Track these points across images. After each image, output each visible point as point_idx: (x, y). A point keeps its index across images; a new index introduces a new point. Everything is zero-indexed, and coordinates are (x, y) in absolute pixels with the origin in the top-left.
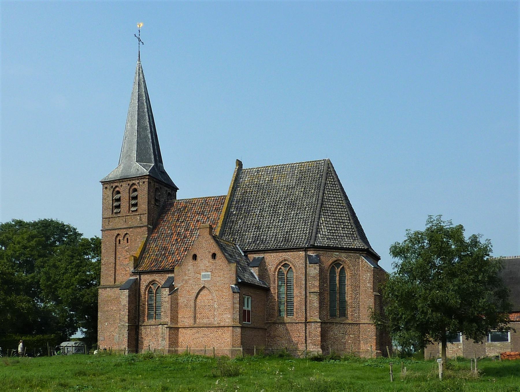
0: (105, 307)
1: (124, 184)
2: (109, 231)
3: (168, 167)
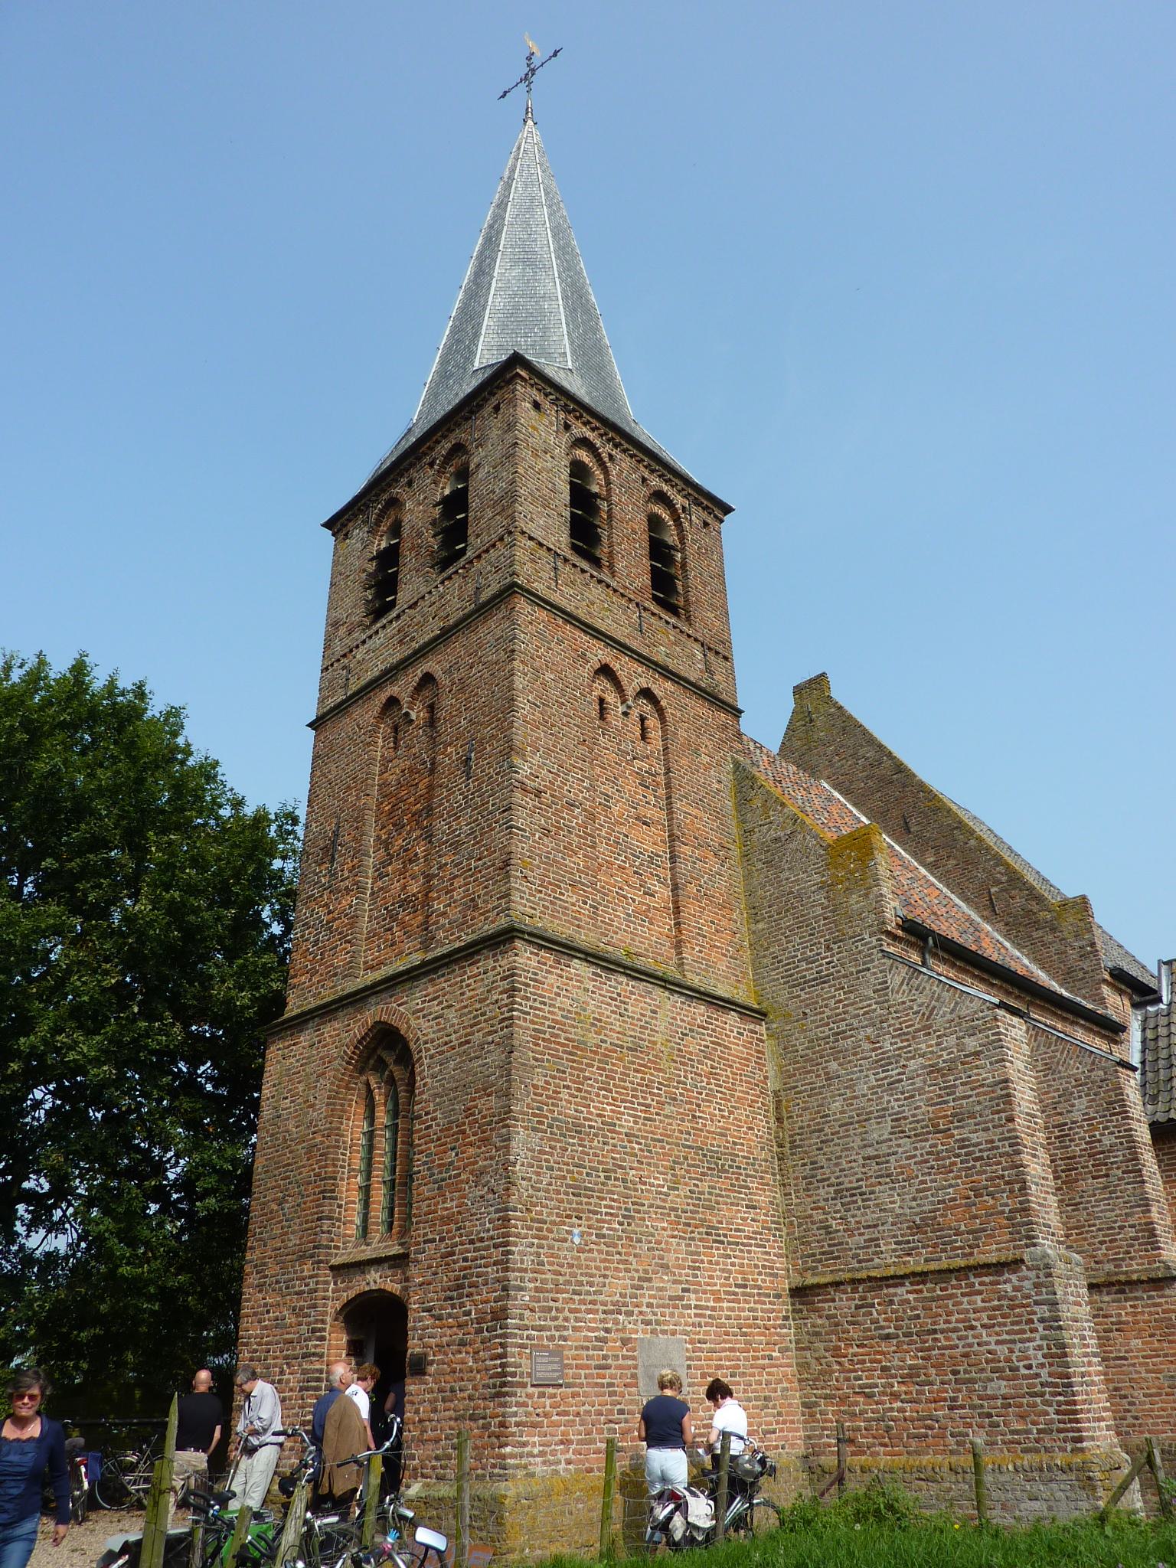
0: (564, 1094)
2: (560, 622)
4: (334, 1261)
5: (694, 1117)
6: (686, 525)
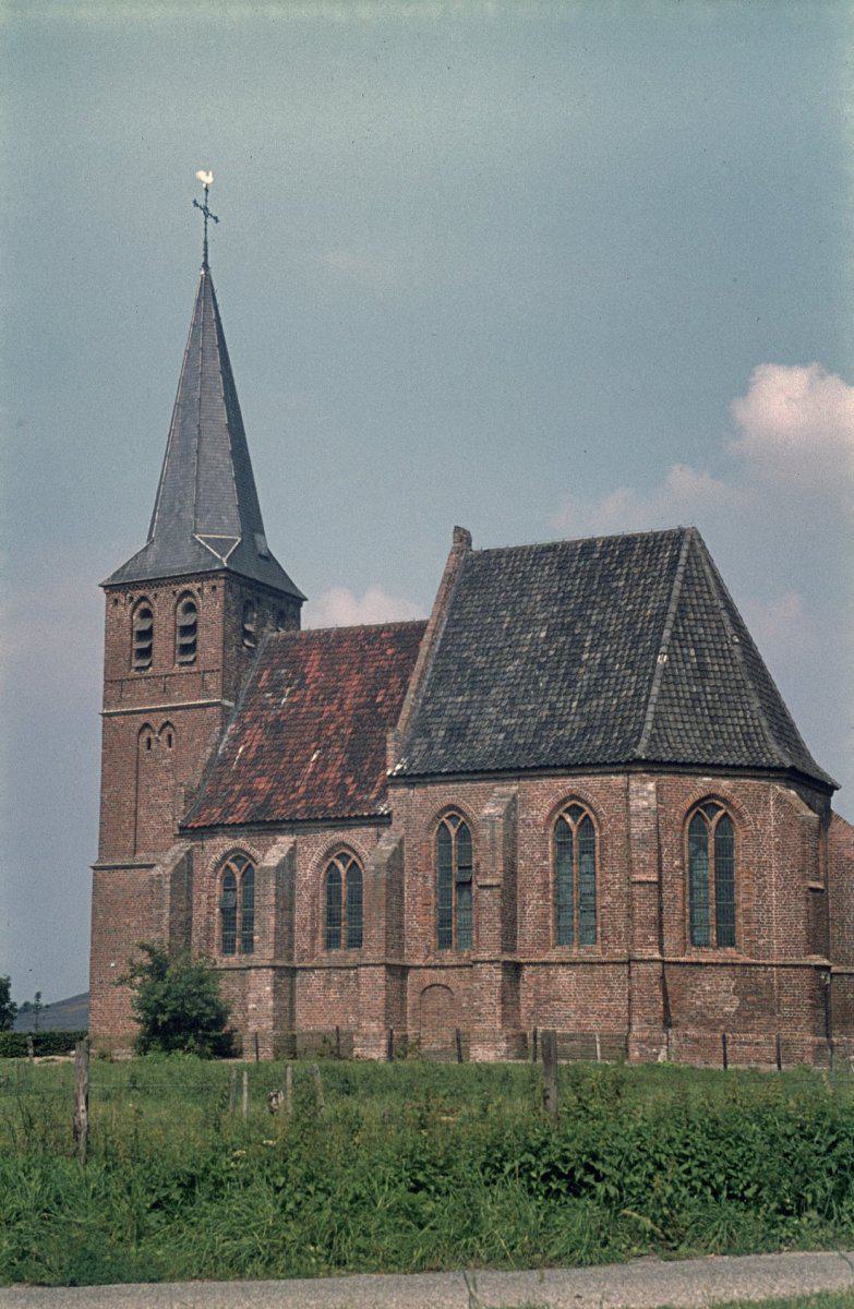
1: (163, 593)
3: (276, 541)
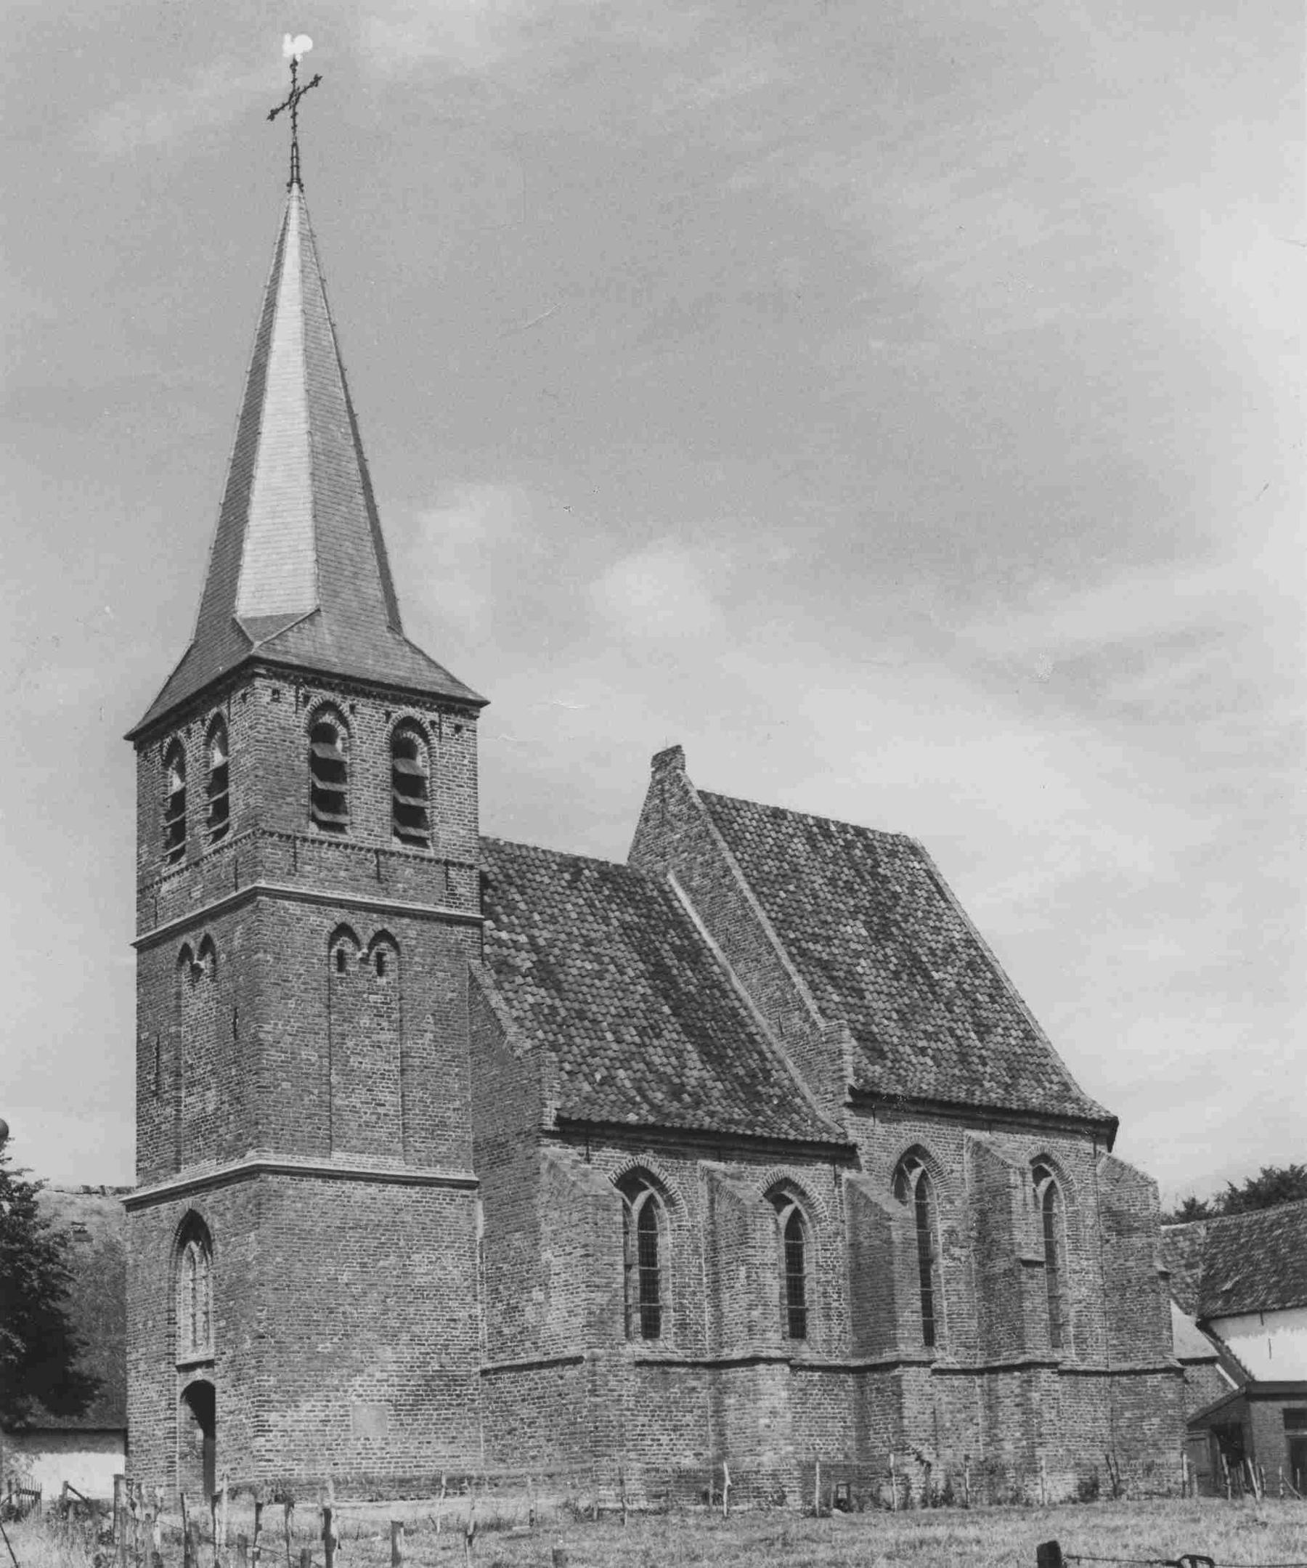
4: (178, 1363)
5: (404, 1265)
6: (435, 741)
